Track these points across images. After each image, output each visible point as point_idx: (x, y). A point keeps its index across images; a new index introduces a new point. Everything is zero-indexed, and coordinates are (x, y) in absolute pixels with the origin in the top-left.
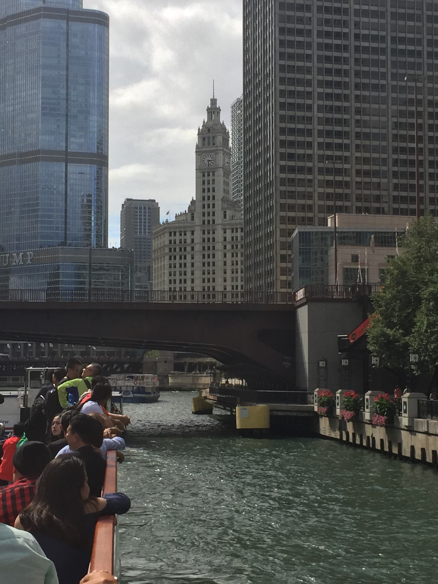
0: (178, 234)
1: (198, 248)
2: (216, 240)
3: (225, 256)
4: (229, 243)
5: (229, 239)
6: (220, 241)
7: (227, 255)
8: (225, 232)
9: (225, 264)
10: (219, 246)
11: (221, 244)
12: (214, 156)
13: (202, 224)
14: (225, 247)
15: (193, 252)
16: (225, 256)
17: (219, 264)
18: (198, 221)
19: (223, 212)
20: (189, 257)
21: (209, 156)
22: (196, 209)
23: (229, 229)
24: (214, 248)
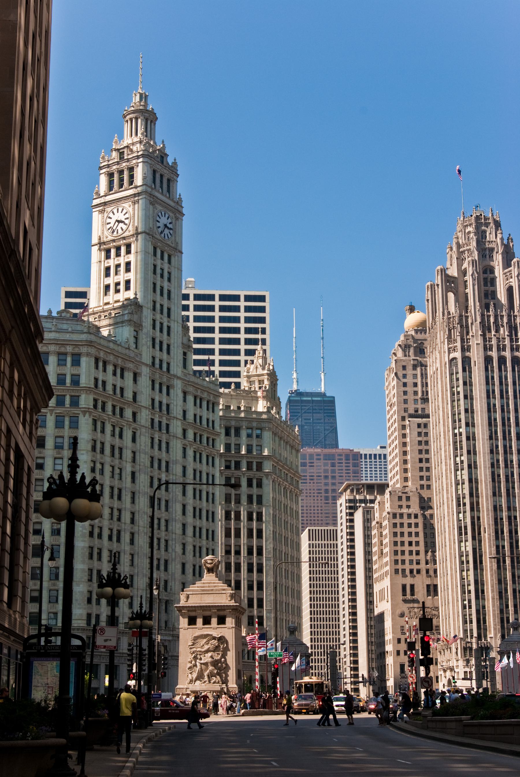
0: (110, 368)
1: (144, 417)
5: (190, 417)
8: (185, 400)
11: (179, 423)
12: (174, 221)
15: (134, 425)
20: (128, 435)
22: (144, 324)
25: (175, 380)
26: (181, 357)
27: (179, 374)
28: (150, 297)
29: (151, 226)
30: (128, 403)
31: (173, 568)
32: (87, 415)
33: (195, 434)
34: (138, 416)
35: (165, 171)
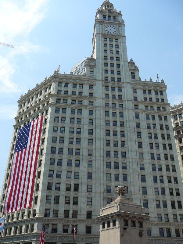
0: (70, 86)
1: (99, 102)
2: (125, 97)
3: (137, 116)
4: (141, 102)
6: (131, 100)
7: (141, 115)
9: (138, 126)
10: (129, 105)
11: (131, 102)
12: (118, 28)
13: (104, 79)
14: (136, 107)
16: (137, 116)
17: (130, 124)
18: (99, 74)
19: (130, 72)
20: (85, 113)
21: (112, 26)
22: (96, 65)
23: (141, 89)
24: (121, 105)
25: (125, 84)
26: (130, 75)
27: (128, 81)
28: (104, 55)
29: (101, 30)
30: (85, 98)
31: (131, 178)
32: (52, 105)
33: (147, 107)
34: (94, 103)
35: (111, 14)
